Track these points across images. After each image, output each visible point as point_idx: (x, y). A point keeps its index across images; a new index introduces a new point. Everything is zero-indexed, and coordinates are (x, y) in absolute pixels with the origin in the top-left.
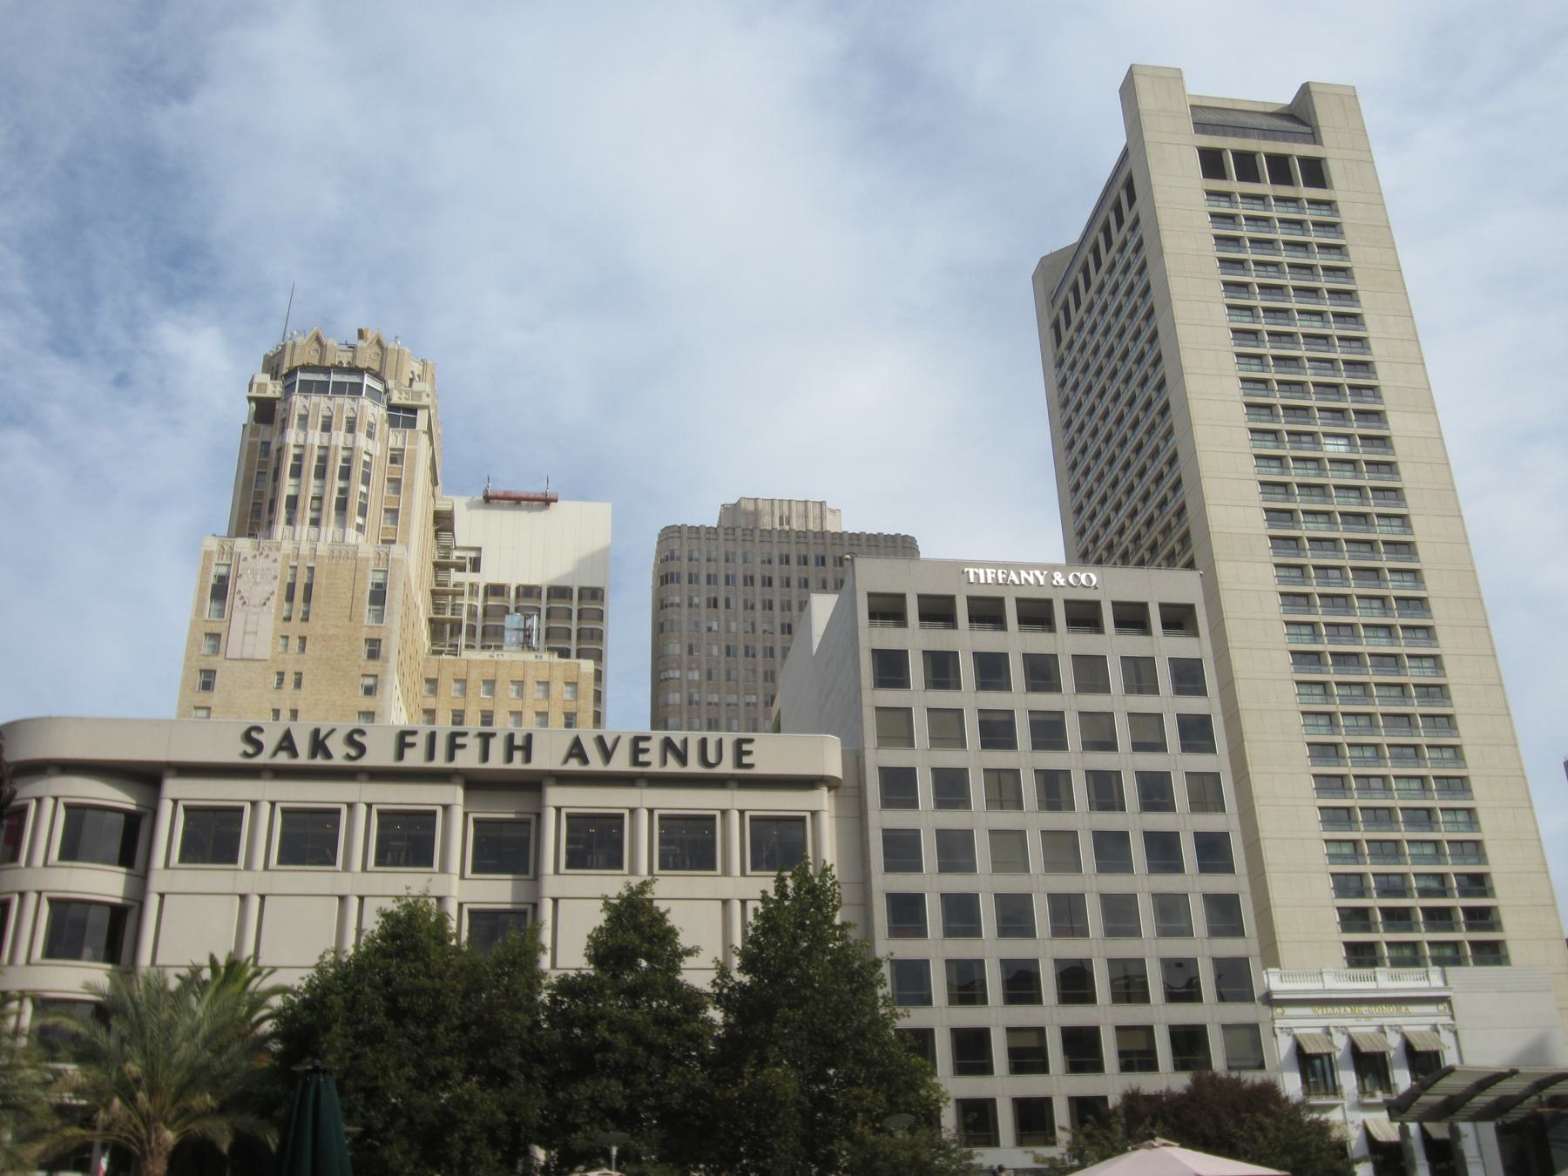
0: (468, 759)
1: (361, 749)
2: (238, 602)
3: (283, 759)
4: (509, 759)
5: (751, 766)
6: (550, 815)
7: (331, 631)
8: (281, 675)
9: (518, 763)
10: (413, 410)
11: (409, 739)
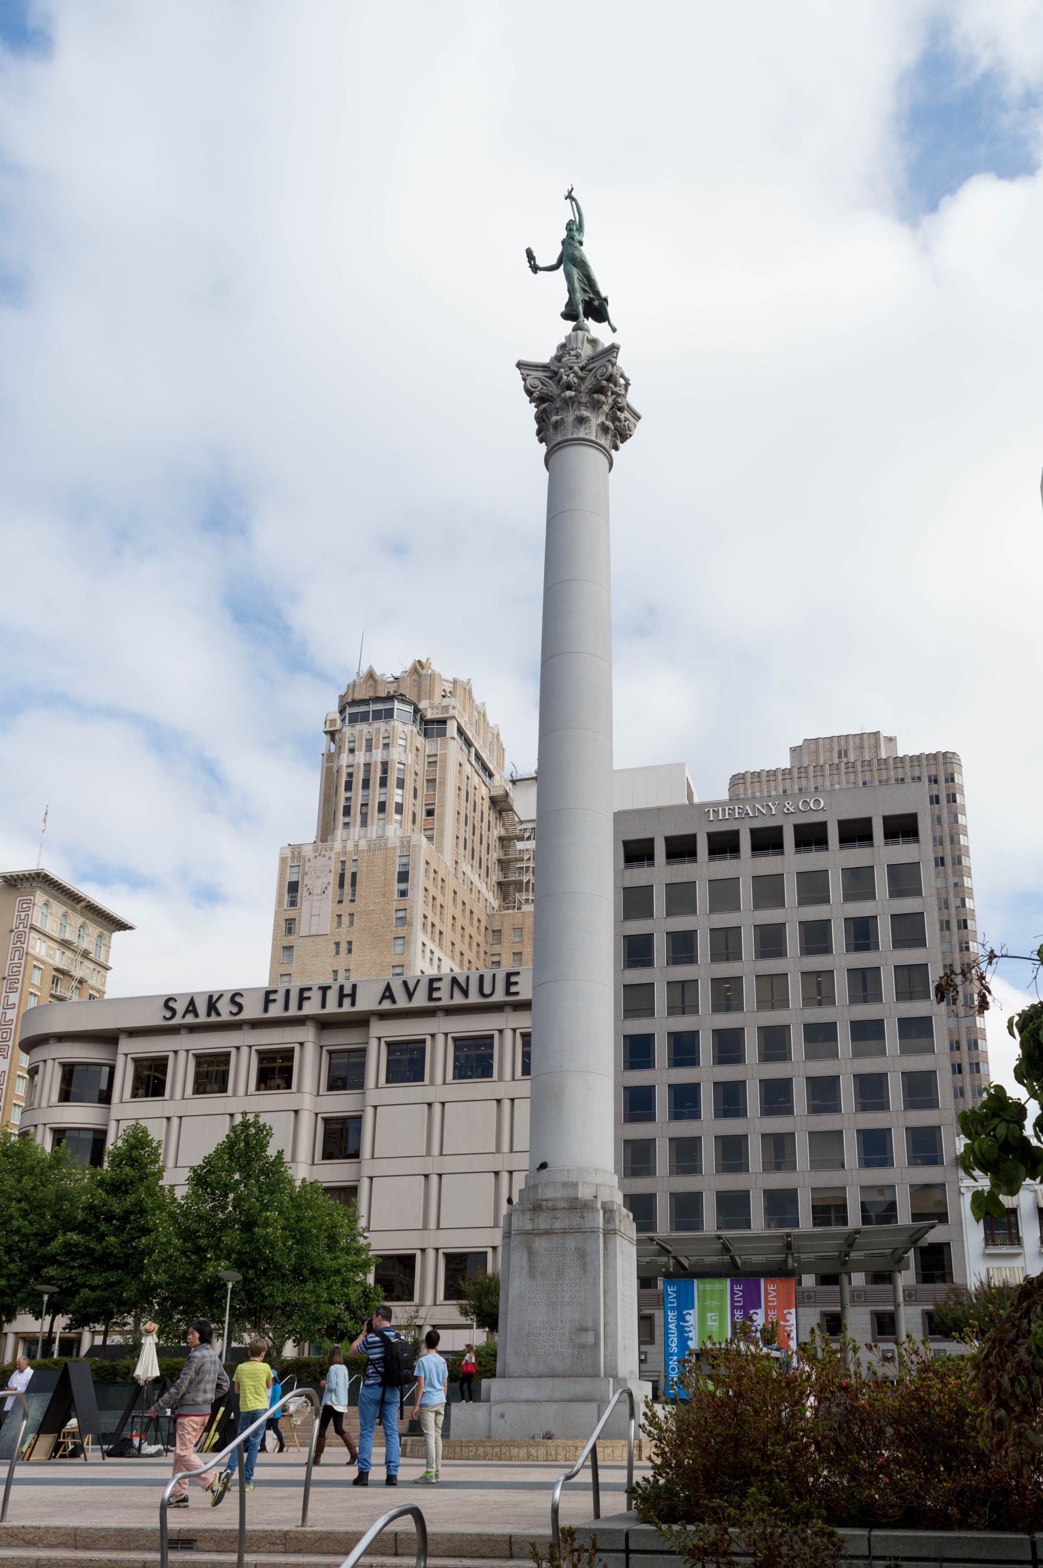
0: (312, 1008)
1: (240, 1008)
2: (305, 893)
3: (190, 1019)
4: (340, 1005)
5: (517, 993)
6: (373, 1044)
7: (372, 907)
8: (337, 944)
9: (347, 1007)
10: (443, 722)
11: (272, 997)
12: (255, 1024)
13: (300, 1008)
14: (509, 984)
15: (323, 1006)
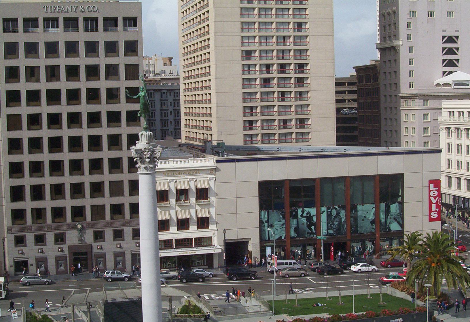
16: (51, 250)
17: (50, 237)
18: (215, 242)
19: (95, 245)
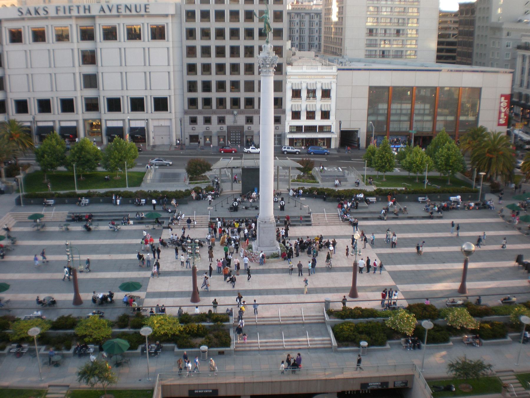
0: (75, 13)
4: (85, 12)
9: (87, 14)
12: (53, 18)
13: (70, 13)
14: (146, 8)
15: (79, 12)
16: (215, 127)
17: (214, 119)
18: (333, 130)
19: (246, 127)
